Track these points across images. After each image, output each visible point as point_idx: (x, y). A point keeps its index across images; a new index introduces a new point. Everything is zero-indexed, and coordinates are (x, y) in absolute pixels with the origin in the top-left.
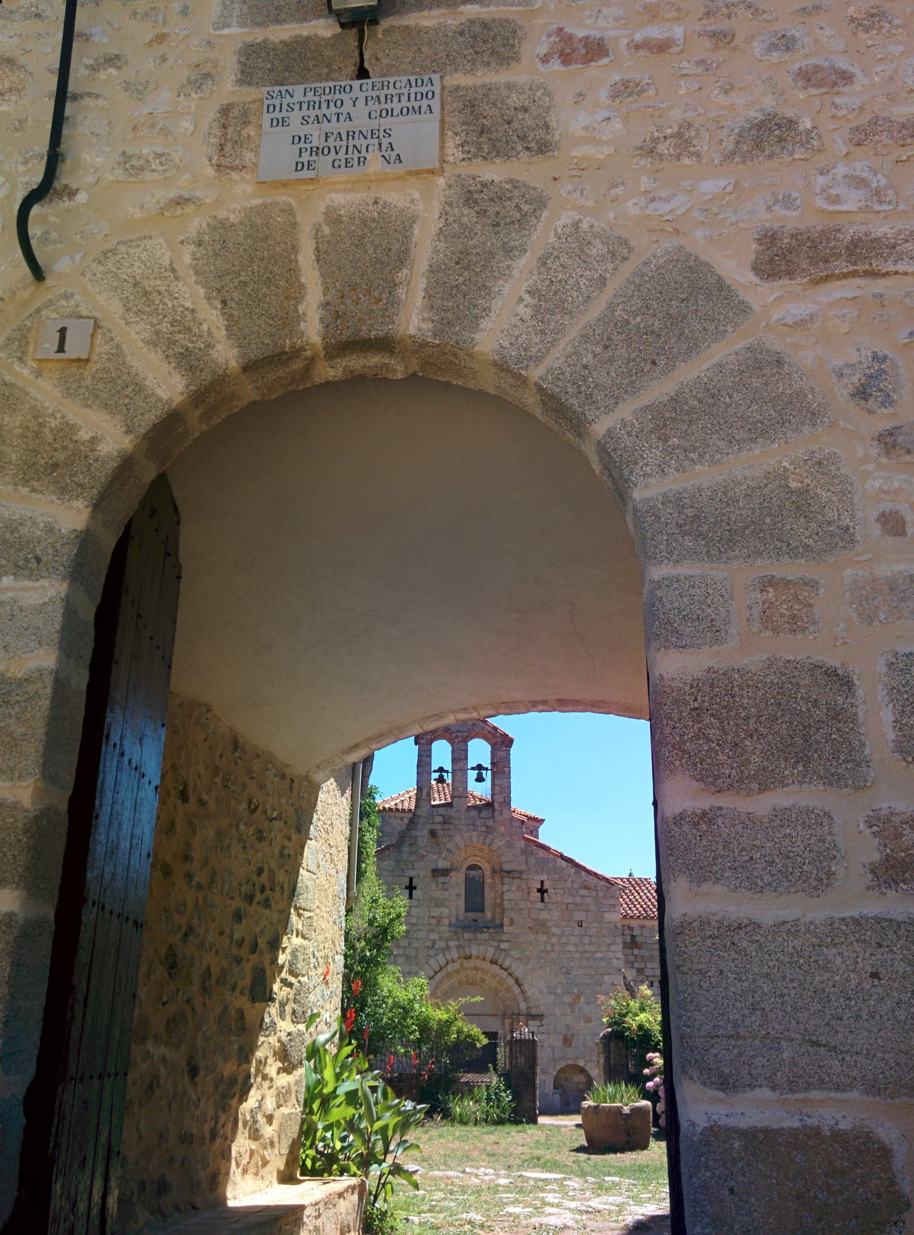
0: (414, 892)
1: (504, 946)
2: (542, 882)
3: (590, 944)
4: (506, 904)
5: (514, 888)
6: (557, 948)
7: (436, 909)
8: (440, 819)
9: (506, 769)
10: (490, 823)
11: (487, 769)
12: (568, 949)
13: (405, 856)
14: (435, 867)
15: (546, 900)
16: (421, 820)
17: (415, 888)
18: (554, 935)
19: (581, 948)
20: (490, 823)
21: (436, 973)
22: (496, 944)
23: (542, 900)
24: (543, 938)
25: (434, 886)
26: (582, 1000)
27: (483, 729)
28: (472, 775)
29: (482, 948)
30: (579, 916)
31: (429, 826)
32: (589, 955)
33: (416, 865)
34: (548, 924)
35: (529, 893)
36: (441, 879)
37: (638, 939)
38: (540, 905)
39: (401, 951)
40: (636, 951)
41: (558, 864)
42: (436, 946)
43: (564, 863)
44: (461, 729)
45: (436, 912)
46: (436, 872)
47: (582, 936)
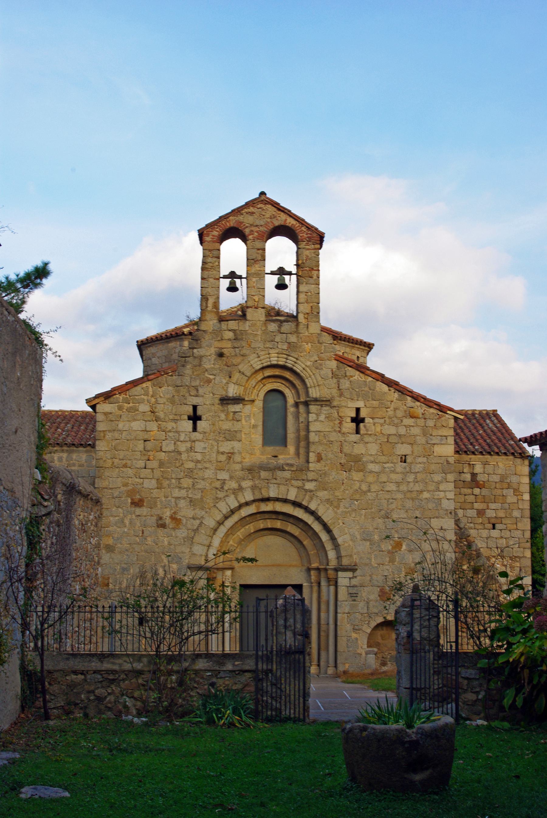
1: (309, 486)
2: (358, 410)
3: (416, 481)
4: (313, 437)
5: (322, 417)
6: (374, 488)
8: (230, 335)
9: (314, 273)
10: (293, 339)
11: (290, 274)
13: (187, 380)
14: (224, 393)
17: (200, 418)
18: (371, 472)
19: (404, 488)
20: (293, 339)
22: (300, 483)
23: (358, 432)
24: (357, 476)
25: (223, 416)
26: (404, 547)
28: (271, 281)
29: (283, 488)
30: (403, 449)
32: (414, 495)
33: (201, 391)
34: (364, 459)
35: (340, 423)
36: (233, 408)
37: (480, 478)
38: (356, 437)
39: (183, 493)
40: (477, 491)
41: (377, 389)
42: (226, 488)
43: (385, 388)
44: (258, 222)
45: (226, 447)
46: (225, 401)
47: (405, 474)
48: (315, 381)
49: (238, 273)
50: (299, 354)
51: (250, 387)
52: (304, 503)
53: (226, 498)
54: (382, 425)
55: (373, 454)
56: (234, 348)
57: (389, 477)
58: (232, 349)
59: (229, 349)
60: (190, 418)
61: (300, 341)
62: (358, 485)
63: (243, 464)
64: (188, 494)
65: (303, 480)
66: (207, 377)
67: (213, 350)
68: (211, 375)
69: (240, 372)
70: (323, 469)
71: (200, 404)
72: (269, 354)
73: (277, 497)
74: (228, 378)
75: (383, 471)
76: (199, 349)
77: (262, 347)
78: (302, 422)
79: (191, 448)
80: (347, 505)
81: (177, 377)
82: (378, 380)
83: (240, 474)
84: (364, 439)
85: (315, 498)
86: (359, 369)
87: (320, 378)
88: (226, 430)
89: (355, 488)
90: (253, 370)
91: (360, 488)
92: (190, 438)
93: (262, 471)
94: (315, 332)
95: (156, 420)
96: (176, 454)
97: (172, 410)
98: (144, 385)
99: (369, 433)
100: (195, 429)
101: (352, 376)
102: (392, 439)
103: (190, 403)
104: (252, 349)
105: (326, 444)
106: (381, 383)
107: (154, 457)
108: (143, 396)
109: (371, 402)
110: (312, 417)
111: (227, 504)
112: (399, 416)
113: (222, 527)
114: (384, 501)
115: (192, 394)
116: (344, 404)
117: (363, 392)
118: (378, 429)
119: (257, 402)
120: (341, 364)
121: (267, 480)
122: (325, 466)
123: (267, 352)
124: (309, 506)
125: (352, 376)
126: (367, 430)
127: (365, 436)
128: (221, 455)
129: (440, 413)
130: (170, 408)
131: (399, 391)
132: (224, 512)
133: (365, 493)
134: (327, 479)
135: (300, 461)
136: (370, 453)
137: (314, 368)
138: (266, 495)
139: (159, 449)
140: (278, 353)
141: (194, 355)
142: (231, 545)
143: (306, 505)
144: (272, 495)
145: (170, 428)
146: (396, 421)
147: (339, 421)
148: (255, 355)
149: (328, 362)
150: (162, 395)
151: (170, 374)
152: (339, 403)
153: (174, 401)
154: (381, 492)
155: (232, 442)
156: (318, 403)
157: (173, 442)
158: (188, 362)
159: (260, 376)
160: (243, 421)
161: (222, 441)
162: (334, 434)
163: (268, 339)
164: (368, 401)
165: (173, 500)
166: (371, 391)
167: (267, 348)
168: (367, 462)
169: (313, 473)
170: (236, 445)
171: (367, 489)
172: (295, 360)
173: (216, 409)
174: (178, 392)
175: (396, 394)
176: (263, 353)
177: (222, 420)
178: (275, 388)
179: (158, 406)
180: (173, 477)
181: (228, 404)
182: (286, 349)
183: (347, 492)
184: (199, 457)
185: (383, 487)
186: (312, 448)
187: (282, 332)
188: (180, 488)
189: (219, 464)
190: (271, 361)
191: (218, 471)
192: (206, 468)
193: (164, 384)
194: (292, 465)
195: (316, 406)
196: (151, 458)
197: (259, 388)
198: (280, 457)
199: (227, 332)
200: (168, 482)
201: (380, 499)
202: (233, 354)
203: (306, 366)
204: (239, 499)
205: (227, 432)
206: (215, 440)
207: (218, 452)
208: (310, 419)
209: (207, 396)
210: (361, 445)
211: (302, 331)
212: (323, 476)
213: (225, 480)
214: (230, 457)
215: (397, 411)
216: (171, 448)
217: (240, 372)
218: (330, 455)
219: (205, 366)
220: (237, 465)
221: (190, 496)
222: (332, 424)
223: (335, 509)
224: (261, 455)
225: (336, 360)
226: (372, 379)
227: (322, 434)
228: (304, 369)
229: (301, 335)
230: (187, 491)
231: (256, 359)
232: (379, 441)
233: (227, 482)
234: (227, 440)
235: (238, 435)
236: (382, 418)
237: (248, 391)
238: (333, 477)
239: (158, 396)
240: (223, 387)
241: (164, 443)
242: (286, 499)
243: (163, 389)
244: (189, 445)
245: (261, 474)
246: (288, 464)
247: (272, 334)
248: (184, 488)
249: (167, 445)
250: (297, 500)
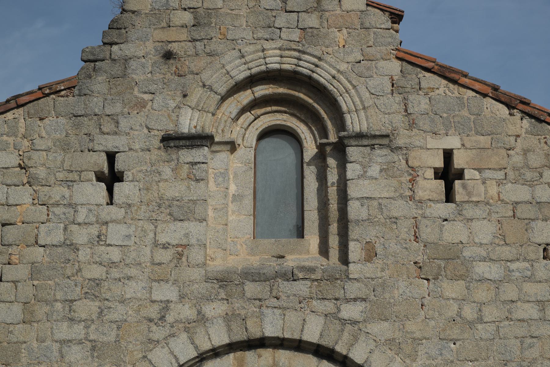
0: (117, 186)
2: (448, 155)
5: (374, 170)
6: (490, 313)
7: (172, 226)
8: (187, 17)
10: (311, 21)
12: (520, 314)
14: (170, 128)
16: (137, 21)
20: (311, 21)
22: (330, 307)
23: (449, 197)
25: (167, 171)
29: (293, 318)
31: (160, 35)
33: (124, 124)
34: (467, 253)
35: (413, 181)
39: (78, 331)
41: (486, 112)
42: (170, 318)
48: (357, 99)
50: (324, 48)
51: (226, 118)
52: (340, 349)
53: (171, 341)
54: (499, 183)
55: (484, 241)
56: (194, 40)
57: (520, 290)
58: (190, 44)
59: (183, 44)
60: (100, 177)
61: (325, 24)
62: (455, 307)
63: (208, 269)
64: (87, 334)
65: (336, 299)
66: (136, 97)
67: (150, 46)
68: (146, 93)
69: (204, 86)
70: (379, 275)
71: (122, 149)
72: (263, 50)
73: (281, 336)
74: (179, 99)
75: (507, 278)
76: (122, 46)
77: (250, 37)
78: (333, 184)
79: (99, 237)
80: (434, 352)
81: (76, 98)
82: (485, 95)
83: (202, 288)
84: (464, 212)
85: (362, 338)
86: (447, 74)
87: (368, 94)
88: (173, 199)
89: (450, 314)
90: (232, 83)
91: (459, 315)
92: (97, 216)
93: (248, 283)
94: (354, 7)
95: (28, 182)
96: (67, 250)
97: (63, 162)
98: (9, 115)
99: (474, 199)
100: (111, 202)
101: (433, 89)
102: (524, 211)
103: (101, 148)
104: (228, 42)
105: (384, 225)
106: (494, 102)
107: (21, 256)
108: (5, 138)
109: (474, 138)
110: (352, 170)
111: (172, 353)
112: (535, 166)
114: (513, 341)
115: (105, 129)
116: (417, 143)
117: (456, 119)
118: (493, 190)
119: (240, 152)
120: (410, 67)
121: (260, 300)
122: (383, 270)
123: (259, 47)
124: (351, 355)
125: (433, 89)
126: (469, 194)
127: (466, 206)
128: (162, 251)
130: (60, 158)
131: (531, 116)
133: (471, 324)
134: (387, 295)
135: (331, 263)
136: (477, 240)
137: (354, 76)
138: (255, 333)
139: (33, 240)
140: (280, 49)
141: (113, 56)
143: (344, 353)
144: (270, 331)
145: (58, 198)
146: (529, 175)
147: (409, 178)
148: (236, 53)
149: (382, 63)
150: (44, 134)
151: (63, 93)
152: (408, 141)
153: (68, 144)
154: (507, 323)
155: (186, 224)
156: (365, 142)
157: (62, 225)
158: (100, 69)
159: (246, 97)
160: (212, 184)
161: (165, 222)
162: (401, 202)
163: (262, 23)
164: (468, 135)
165: (56, 347)
166: (472, 117)
167: (259, 39)
168: (473, 260)
169: (357, 285)
170: (193, 227)
171: (476, 316)
172: (315, 60)
173: (154, 157)
174: (77, 126)
175: (525, 121)
176: (251, 48)
177: (166, 180)
178: (278, 122)
179: (35, 156)
180: (58, 297)
181: (178, 147)
182: (298, 40)
183: (432, 323)
184: (115, 255)
185: (510, 313)
186: (354, 232)
187: (288, 9)
188: (72, 320)
189: (156, 268)
190: (266, 64)
191: (155, 284)
192: (129, 278)
193: (49, 112)
194: (312, 270)
195: (361, 149)
196: (14, 259)
197: (247, 123)
198: (288, 257)
199: (180, 13)
200: (46, 309)
201: (505, 338)
202: (190, 53)
203: (339, 71)
204: (197, 342)
205: (175, 203)
206: (150, 220)
207: (156, 244)
208: (350, 174)
209: (136, 133)
210: (459, 225)
211: (330, 7)
212: (379, 289)
213: (168, 301)
214: (181, 255)
215: (531, 156)
216: (58, 237)
217: (204, 86)
218: (393, 247)
219: (134, 76)
220: (196, 270)
221: (92, 337)
222: (394, 182)
223: (408, 361)
224: (248, 254)
225: (398, 58)
226: (474, 94)
227: (375, 203)
228: (334, 77)
229: (327, 14)
230: (87, 327)
231: (238, 61)
232: (494, 217)
233: (172, 306)
234: (175, 220)
235: (199, 209)
236: (500, 169)
237: (222, 126)
238: (401, 291)
239: (36, 136)
240: (169, 116)
241: (43, 227)
242: (300, 341)
243: (46, 121)
244: (94, 230)
245: (246, 288)
246: (302, 269)
247: (269, 13)
248: (80, 321)
249: (49, 233)
250: (324, 343)
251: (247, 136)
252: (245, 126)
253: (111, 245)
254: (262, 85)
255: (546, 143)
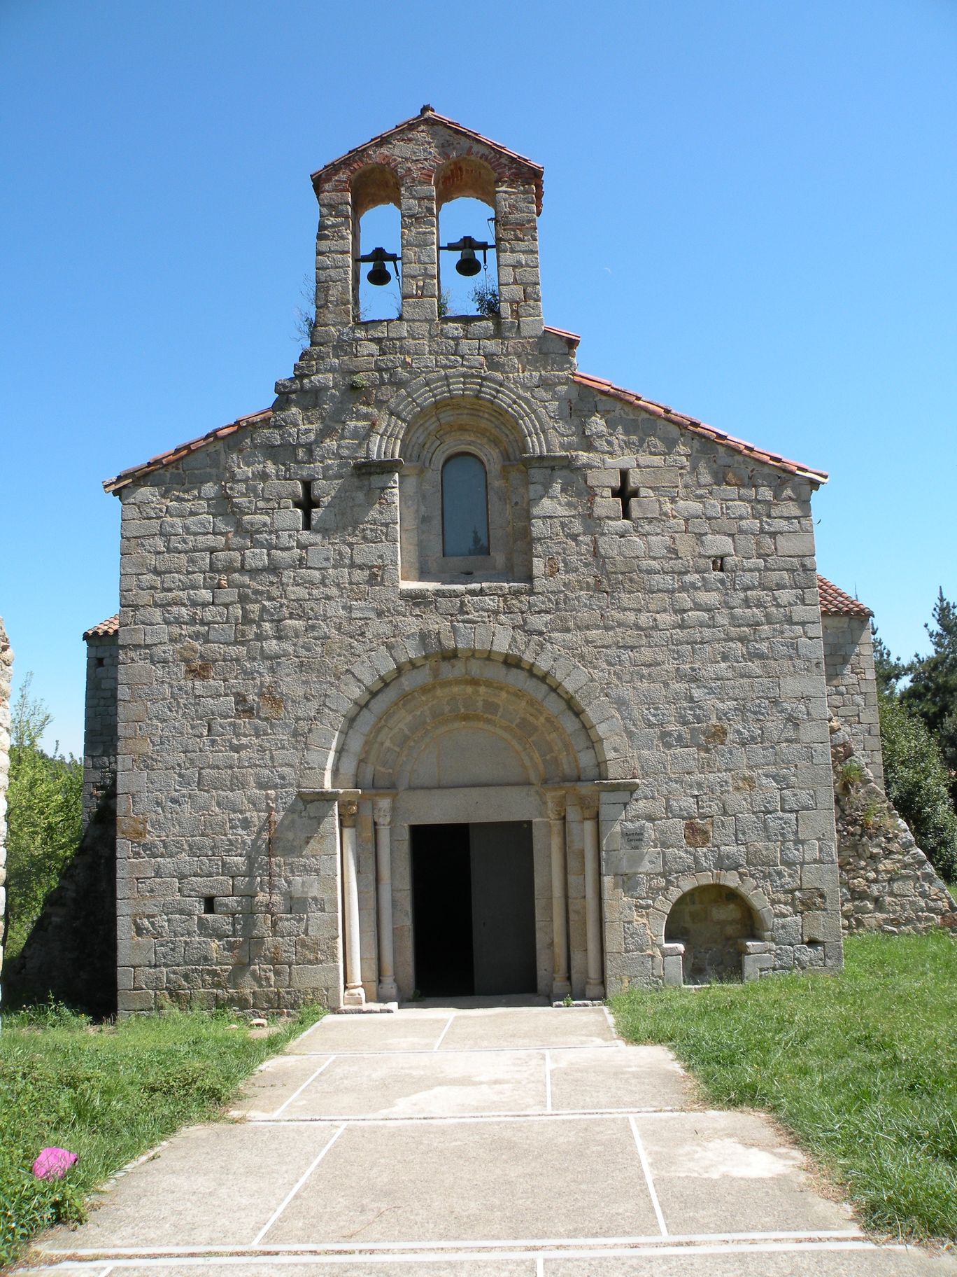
2: (624, 475)
15: (635, 512)
21: (374, 694)
27: (469, 151)
49: (389, 251)
60: (297, 505)
87: (548, 419)
108: (208, 470)
113: (365, 712)
129: (784, 475)
132: (369, 679)
142: (389, 749)
175: (695, 441)
177: (360, 505)
181: (370, 474)
237: (410, 450)
251: (433, 459)
252: (432, 451)
253: (312, 568)
254: (478, 1007)
255: (715, 461)
